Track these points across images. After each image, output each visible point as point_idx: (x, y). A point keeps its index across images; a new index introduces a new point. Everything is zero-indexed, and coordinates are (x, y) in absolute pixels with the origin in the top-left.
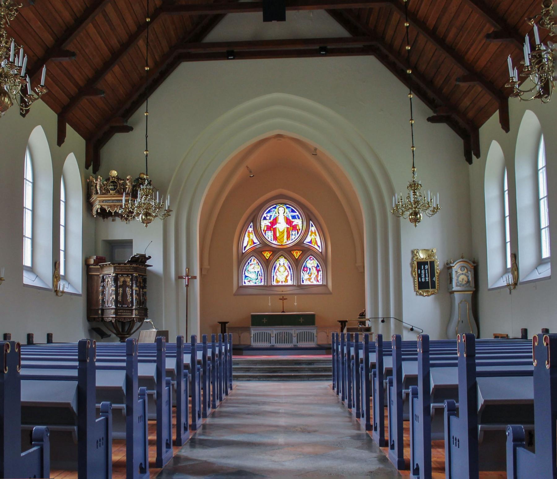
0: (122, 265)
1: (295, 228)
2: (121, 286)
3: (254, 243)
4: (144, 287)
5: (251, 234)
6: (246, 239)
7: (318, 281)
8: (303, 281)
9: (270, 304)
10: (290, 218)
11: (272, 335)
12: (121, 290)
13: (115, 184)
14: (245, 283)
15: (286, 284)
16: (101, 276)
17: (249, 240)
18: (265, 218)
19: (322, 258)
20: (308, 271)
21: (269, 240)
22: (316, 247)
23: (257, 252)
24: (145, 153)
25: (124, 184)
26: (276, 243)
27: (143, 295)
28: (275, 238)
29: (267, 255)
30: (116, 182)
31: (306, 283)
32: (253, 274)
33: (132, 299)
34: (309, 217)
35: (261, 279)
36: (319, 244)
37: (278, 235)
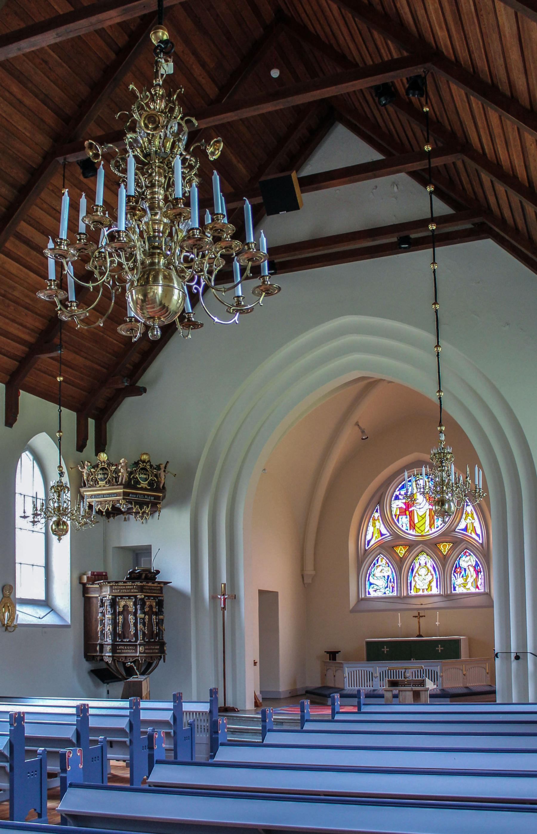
0: (120, 584)
2: (120, 613)
3: (382, 535)
4: (160, 612)
5: (377, 522)
6: (371, 529)
7: (477, 587)
8: (454, 588)
9: (400, 625)
11: (374, 675)
12: (121, 618)
13: (105, 471)
14: (369, 593)
15: (430, 593)
16: (99, 598)
17: (375, 531)
18: (397, 498)
19: (484, 553)
20: (463, 572)
21: (404, 529)
22: (474, 536)
23: (387, 548)
24: (58, 434)
25: (117, 471)
26: (414, 533)
27: (157, 624)
28: (412, 525)
29: (401, 551)
30: (106, 469)
31: (460, 590)
33: (136, 630)
35: (393, 587)
36: (479, 531)
37: (416, 521)
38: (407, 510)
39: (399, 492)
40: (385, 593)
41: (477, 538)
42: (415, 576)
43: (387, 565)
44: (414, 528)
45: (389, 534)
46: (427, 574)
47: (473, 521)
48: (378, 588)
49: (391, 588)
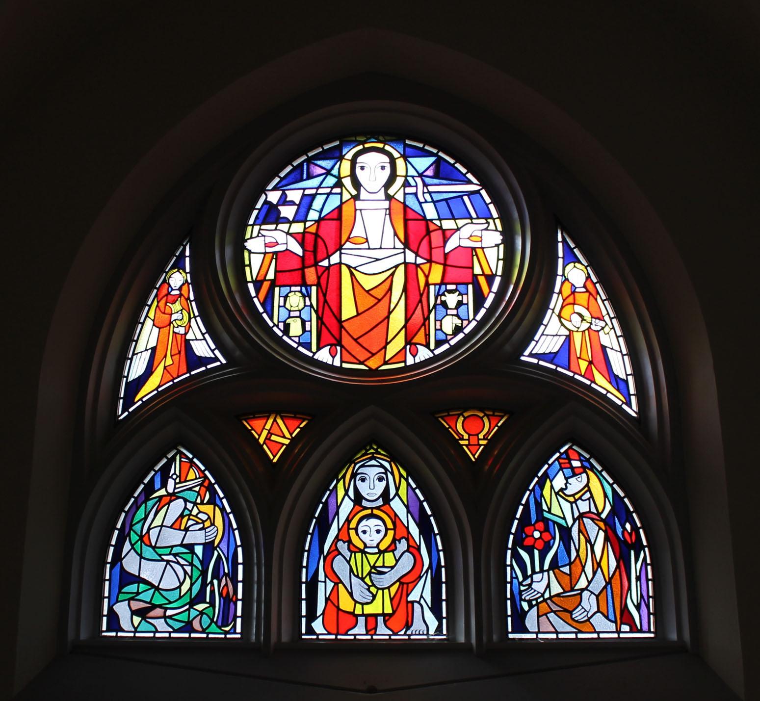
1: (460, 269)
6: (148, 335)
7: (625, 617)
8: (520, 617)
10: (430, 212)
14: (114, 622)
17: (165, 340)
18: (272, 215)
22: (601, 383)
31: (540, 627)
32: (170, 556)
34: (549, 205)
35: (228, 601)
36: (621, 366)
37: (348, 310)
38: (317, 257)
40: (188, 627)
41: (616, 397)
42: (335, 551)
44: (339, 343)
46: (392, 548)
47: (597, 325)
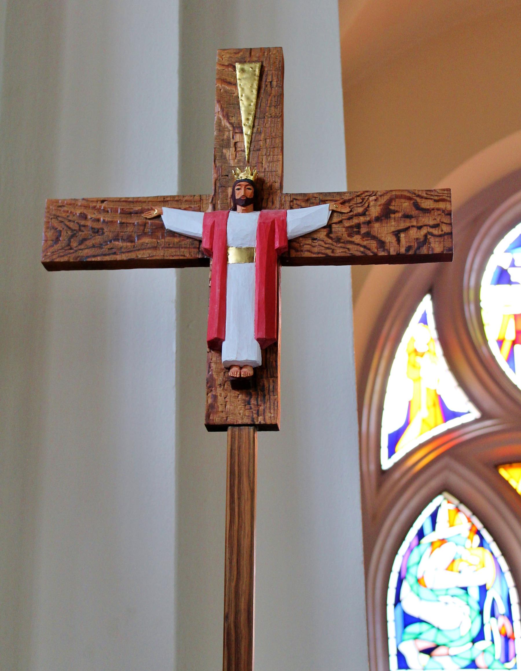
3: (448, 415)
39: (509, 257)
43: (477, 538)
45: (476, 414)
48: (440, 640)
49: (499, 641)
